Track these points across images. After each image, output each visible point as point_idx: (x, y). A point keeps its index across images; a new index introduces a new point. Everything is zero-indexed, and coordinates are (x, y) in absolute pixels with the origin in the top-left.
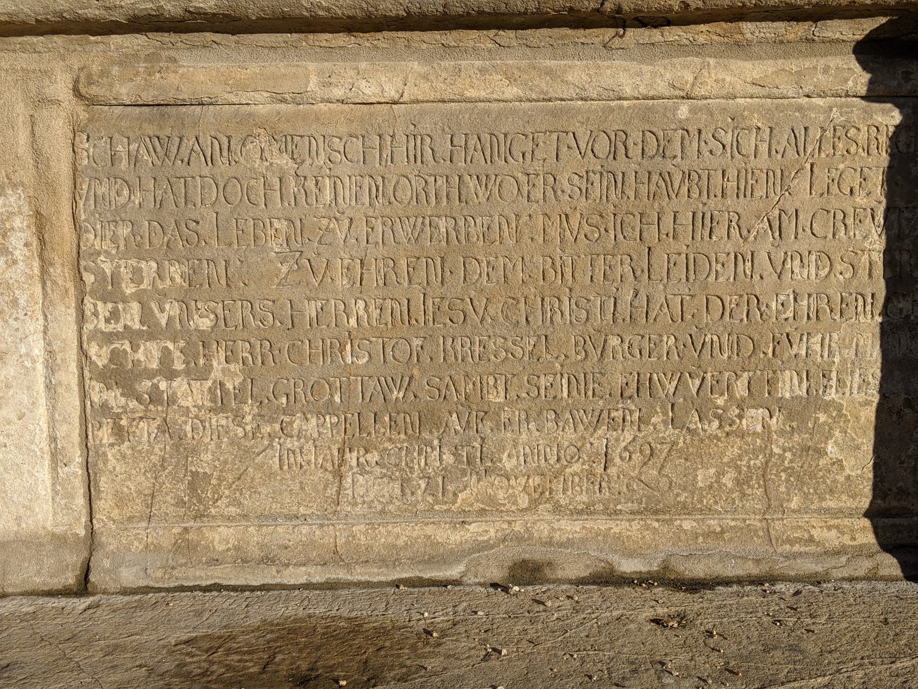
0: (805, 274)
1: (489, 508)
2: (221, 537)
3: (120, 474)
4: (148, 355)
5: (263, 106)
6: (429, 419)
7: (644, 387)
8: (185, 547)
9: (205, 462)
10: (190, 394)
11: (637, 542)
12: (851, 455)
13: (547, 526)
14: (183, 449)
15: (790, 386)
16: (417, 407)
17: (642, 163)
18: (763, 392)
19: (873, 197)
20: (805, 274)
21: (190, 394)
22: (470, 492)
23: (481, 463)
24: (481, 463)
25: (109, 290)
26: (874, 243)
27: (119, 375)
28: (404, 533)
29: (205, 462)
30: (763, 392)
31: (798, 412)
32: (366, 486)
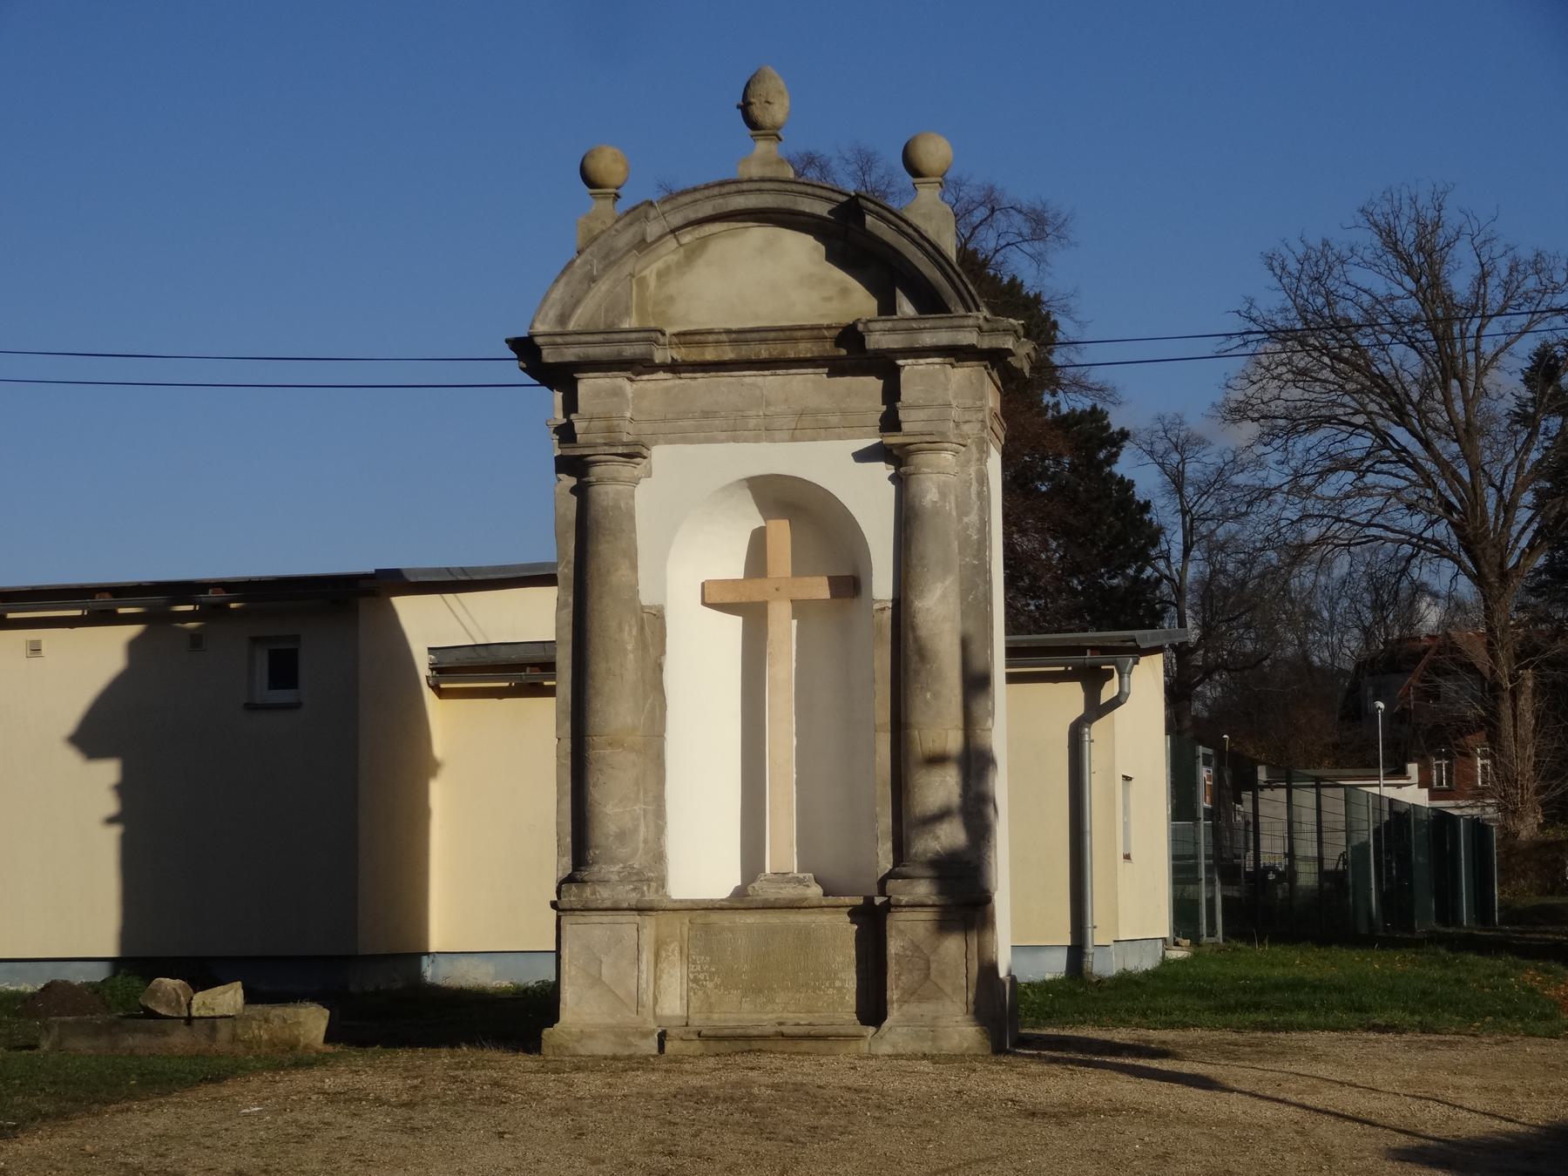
0: (839, 959)
3: (695, 1003)
4: (701, 976)
5: (727, 924)
6: (761, 991)
8: (708, 1019)
9: (713, 1000)
10: (710, 985)
11: (804, 1018)
12: (851, 999)
13: (785, 1015)
14: (708, 997)
15: (838, 984)
16: (757, 988)
18: (832, 986)
21: (710, 985)
22: (769, 1007)
25: (694, 963)
27: (696, 981)
28: (755, 1016)
29: (713, 1000)
30: (832, 986)
31: (840, 989)
32: (746, 1006)
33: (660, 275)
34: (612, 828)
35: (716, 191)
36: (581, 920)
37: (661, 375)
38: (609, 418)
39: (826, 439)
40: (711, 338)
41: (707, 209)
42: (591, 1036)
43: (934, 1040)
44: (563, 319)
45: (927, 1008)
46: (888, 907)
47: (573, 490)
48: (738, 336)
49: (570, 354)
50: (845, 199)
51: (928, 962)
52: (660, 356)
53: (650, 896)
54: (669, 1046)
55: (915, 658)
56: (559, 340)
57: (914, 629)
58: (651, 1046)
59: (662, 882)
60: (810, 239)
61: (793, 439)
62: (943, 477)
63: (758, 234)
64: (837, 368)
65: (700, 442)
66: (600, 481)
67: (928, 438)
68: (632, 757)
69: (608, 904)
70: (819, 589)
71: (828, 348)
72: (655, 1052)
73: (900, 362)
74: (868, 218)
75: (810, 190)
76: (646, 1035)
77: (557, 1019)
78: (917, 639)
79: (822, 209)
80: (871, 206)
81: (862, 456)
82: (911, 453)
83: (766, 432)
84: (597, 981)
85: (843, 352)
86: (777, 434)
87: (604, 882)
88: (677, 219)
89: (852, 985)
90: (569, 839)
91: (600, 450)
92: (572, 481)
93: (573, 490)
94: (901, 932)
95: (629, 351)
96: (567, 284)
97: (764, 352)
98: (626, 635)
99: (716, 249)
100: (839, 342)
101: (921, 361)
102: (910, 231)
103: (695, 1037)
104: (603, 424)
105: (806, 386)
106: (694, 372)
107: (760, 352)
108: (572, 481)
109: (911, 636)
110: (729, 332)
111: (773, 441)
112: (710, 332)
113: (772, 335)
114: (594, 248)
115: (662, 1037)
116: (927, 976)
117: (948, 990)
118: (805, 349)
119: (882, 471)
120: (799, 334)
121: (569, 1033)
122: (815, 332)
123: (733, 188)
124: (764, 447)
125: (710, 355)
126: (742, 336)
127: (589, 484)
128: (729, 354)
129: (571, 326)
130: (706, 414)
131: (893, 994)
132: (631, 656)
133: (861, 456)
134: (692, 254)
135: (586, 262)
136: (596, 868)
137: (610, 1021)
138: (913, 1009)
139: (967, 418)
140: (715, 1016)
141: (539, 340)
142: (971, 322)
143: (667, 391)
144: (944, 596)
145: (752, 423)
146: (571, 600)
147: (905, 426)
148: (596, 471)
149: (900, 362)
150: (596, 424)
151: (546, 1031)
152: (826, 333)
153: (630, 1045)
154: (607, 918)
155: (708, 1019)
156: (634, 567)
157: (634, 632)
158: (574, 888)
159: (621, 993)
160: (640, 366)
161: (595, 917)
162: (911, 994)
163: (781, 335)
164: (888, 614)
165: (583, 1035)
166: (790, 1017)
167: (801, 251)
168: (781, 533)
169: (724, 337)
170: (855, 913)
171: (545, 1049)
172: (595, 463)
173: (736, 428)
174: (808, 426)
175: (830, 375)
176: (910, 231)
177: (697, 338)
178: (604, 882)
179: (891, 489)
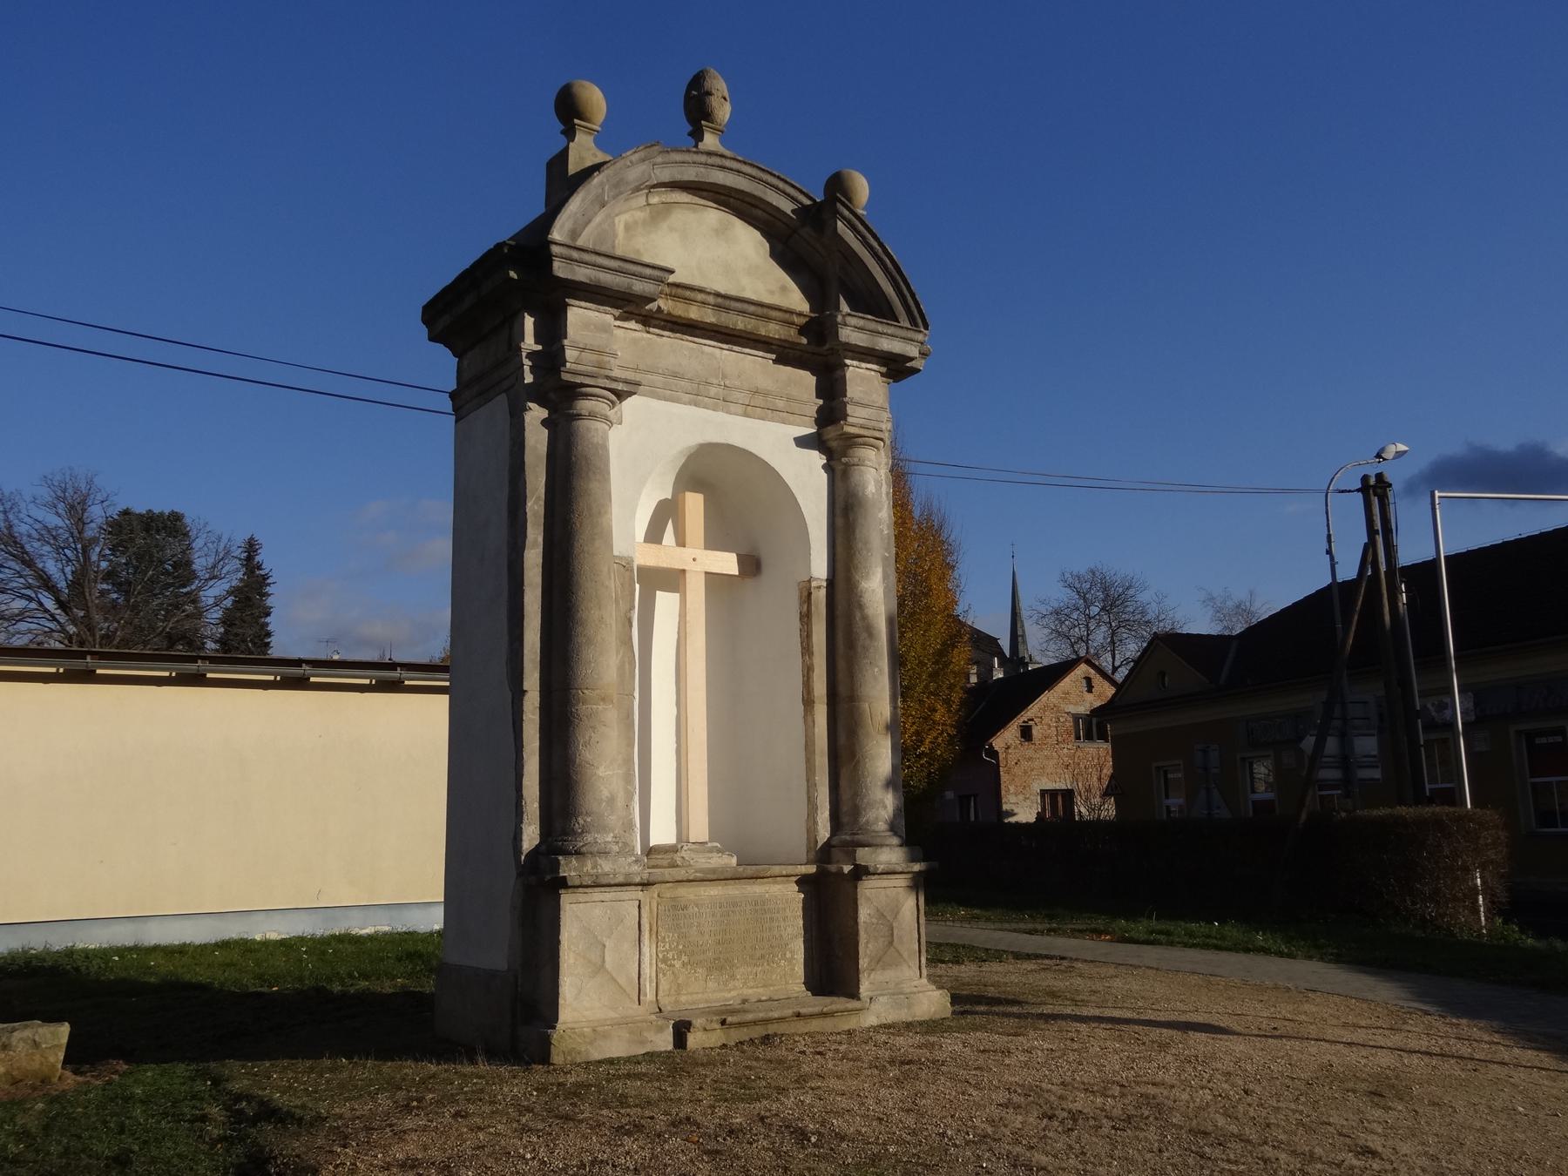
1: (735, 988)
2: (683, 998)
4: (670, 955)
5: (692, 897)
6: (722, 968)
7: (763, 957)
8: (677, 1001)
10: (678, 964)
11: (764, 993)
16: (720, 966)
17: (760, 906)
19: (800, 913)
20: (789, 930)
23: (733, 977)
24: (733, 977)
26: (801, 923)
27: (665, 960)
33: (628, 228)
34: (605, 793)
36: (582, 897)
37: (632, 324)
38: (600, 352)
39: (772, 420)
40: (700, 297)
41: (690, 174)
42: (605, 1036)
43: (909, 1007)
44: (574, 234)
45: (889, 975)
46: (861, 872)
47: (544, 423)
48: (725, 301)
49: (582, 274)
50: (809, 202)
51: (892, 929)
54: (694, 1040)
55: (864, 635)
56: (575, 254)
57: (861, 607)
58: (665, 1041)
60: (757, 234)
61: (746, 415)
63: (713, 216)
64: (785, 355)
65: (666, 399)
66: (592, 415)
69: (620, 879)
70: (727, 563)
71: (791, 334)
72: (670, 1047)
73: (848, 362)
74: (839, 223)
75: (781, 185)
76: (660, 1029)
78: (865, 618)
79: (787, 207)
80: (846, 213)
81: (802, 442)
82: (851, 446)
83: (723, 403)
84: (600, 968)
85: (804, 341)
86: (732, 407)
87: (605, 853)
88: (665, 175)
89: (800, 956)
90: (536, 805)
91: (601, 382)
92: (544, 413)
93: (544, 423)
94: (868, 899)
95: (639, 287)
97: (740, 323)
99: (680, 217)
100: (802, 330)
101: (864, 365)
102: (875, 244)
103: (718, 1026)
104: (594, 357)
105: (753, 366)
106: (663, 328)
107: (728, 323)
108: (544, 413)
109: (858, 615)
110: (718, 295)
111: (728, 412)
112: (701, 291)
113: (752, 308)
115: (681, 1031)
116: (891, 943)
117: (905, 955)
118: (773, 330)
119: (816, 459)
120: (774, 314)
121: (583, 1035)
122: (787, 316)
124: (720, 416)
125: (694, 313)
126: (727, 303)
127: (579, 416)
128: (709, 317)
129: (580, 243)
130: (675, 375)
131: (863, 963)
133: (802, 442)
134: (659, 214)
136: (589, 838)
137: (612, 1014)
138: (879, 976)
140: (683, 998)
141: (555, 249)
142: (920, 337)
143: (635, 341)
145: (713, 391)
146: (540, 539)
147: (850, 419)
148: (584, 405)
149: (848, 362)
150: (587, 356)
152: (796, 319)
153: (643, 1043)
154: (609, 895)
155: (677, 1001)
158: (574, 861)
159: (622, 981)
160: (629, 305)
161: (597, 895)
162: (879, 962)
163: (759, 310)
164: (823, 591)
165: (598, 1033)
166: (748, 992)
167: (748, 243)
168: (694, 503)
169: (711, 299)
170: (803, 882)
171: (557, 1058)
172: (586, 396)
173: (698, 392)
174: (760, 405)
175: (775, 361)
176: (875, 244)
177: (688, 293)
178: (605, 853)
179: (824, 476)
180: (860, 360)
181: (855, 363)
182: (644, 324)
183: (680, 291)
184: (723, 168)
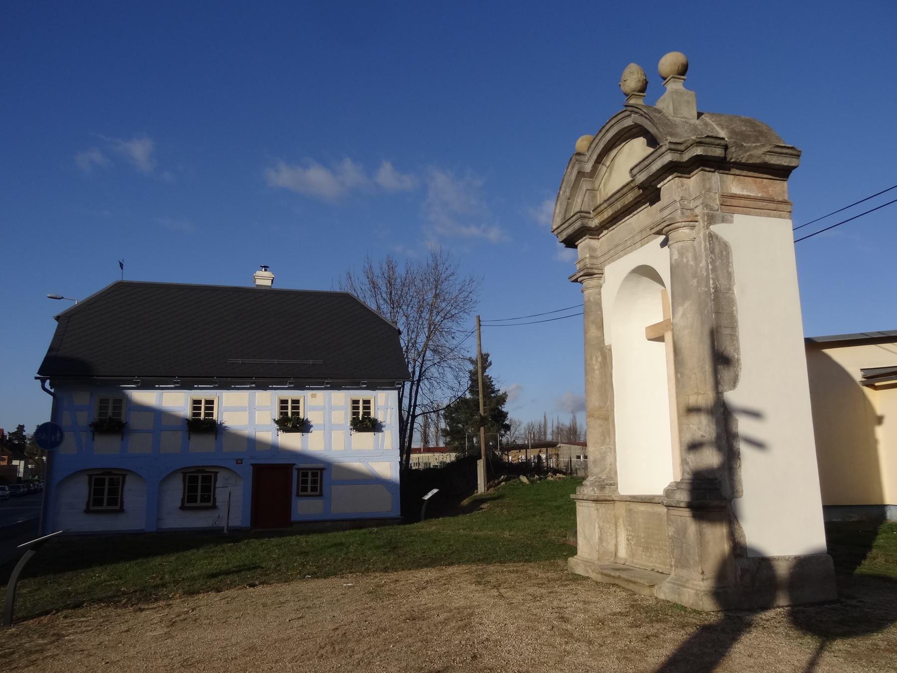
35: (600, 135)
40: (602, 207)
45: (684, 573)
52: (594, 223)
53: (607, 493)
59: (615, 484)
62: (680, 244)
67: (665, 224)
68: (599, 422)
73: (659, 186)
77: (576, 554)
96: (561, 204)
97: (618, 206)
98: (594, 362)
101: (665, 181)
113: (617, 196)
114: (564, 184)
118: (630, 197)
120: (625, 190)
123: (604, 131)
132: (597, 372)
135: (564, 192)
139: (696, 205)
144: (684, 314)
149: (659, 186)
151: (570, 559)
156: (601, 327)
157: (600, 359)
169: (605, 205)
175: (651, 205)
180: (663, 180)
181: (662, 184)
182: (607, 229)
183: (599, 209)
184: (608, 131)
